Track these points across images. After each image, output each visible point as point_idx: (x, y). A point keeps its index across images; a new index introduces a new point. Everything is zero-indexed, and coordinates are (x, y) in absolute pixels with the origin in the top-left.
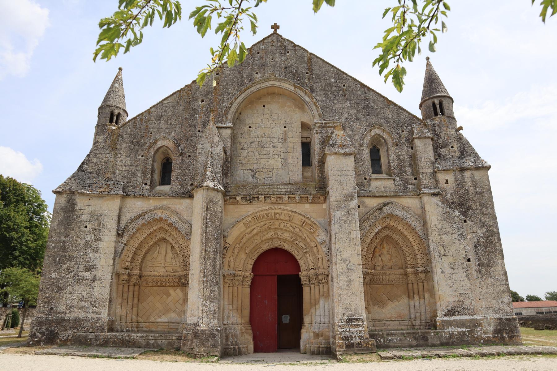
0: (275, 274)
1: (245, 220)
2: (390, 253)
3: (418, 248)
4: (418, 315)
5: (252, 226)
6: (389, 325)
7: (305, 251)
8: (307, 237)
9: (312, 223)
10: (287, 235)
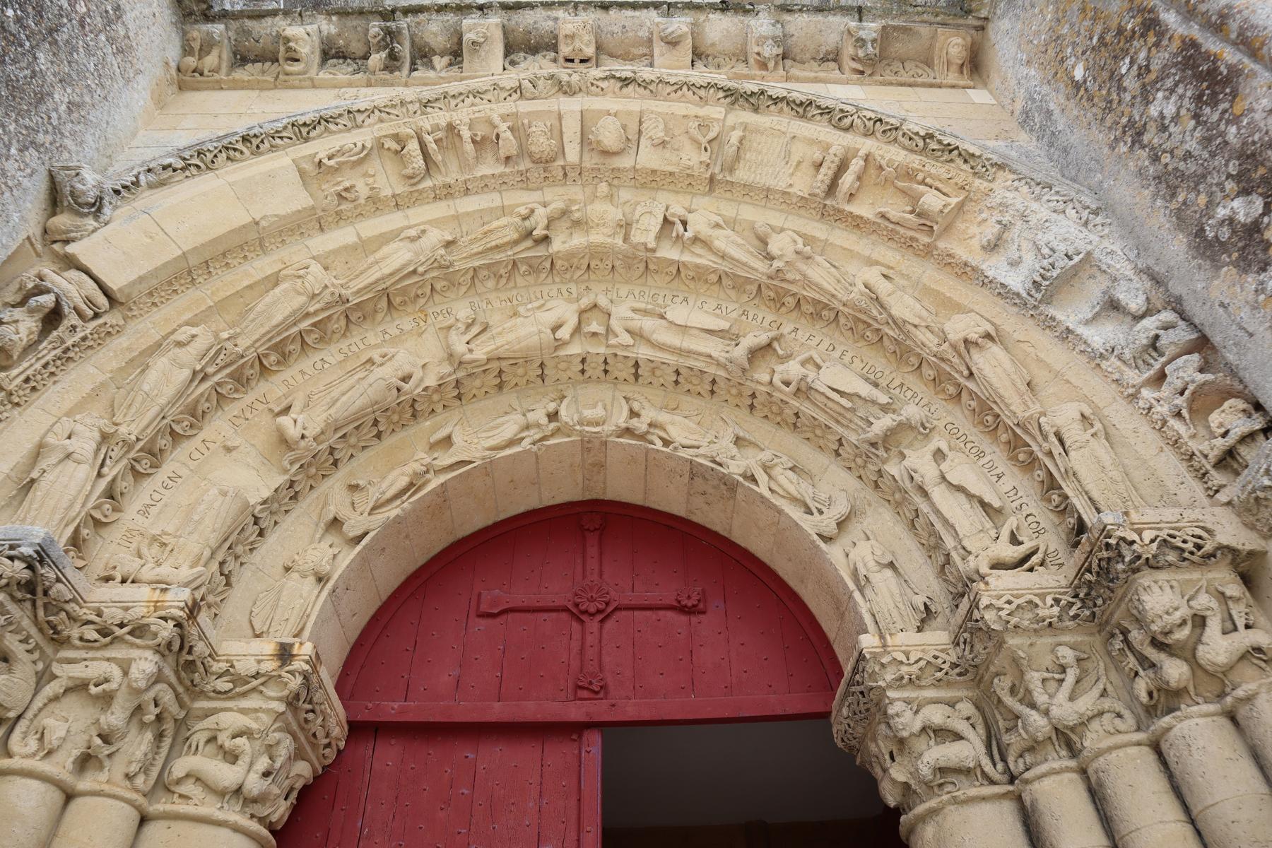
0: (575, 712)
1: (321, 147)
5: (376, 203)
7: (883, 423)
8: (883, 287)
9: (915, 161)
10: (694, 324)
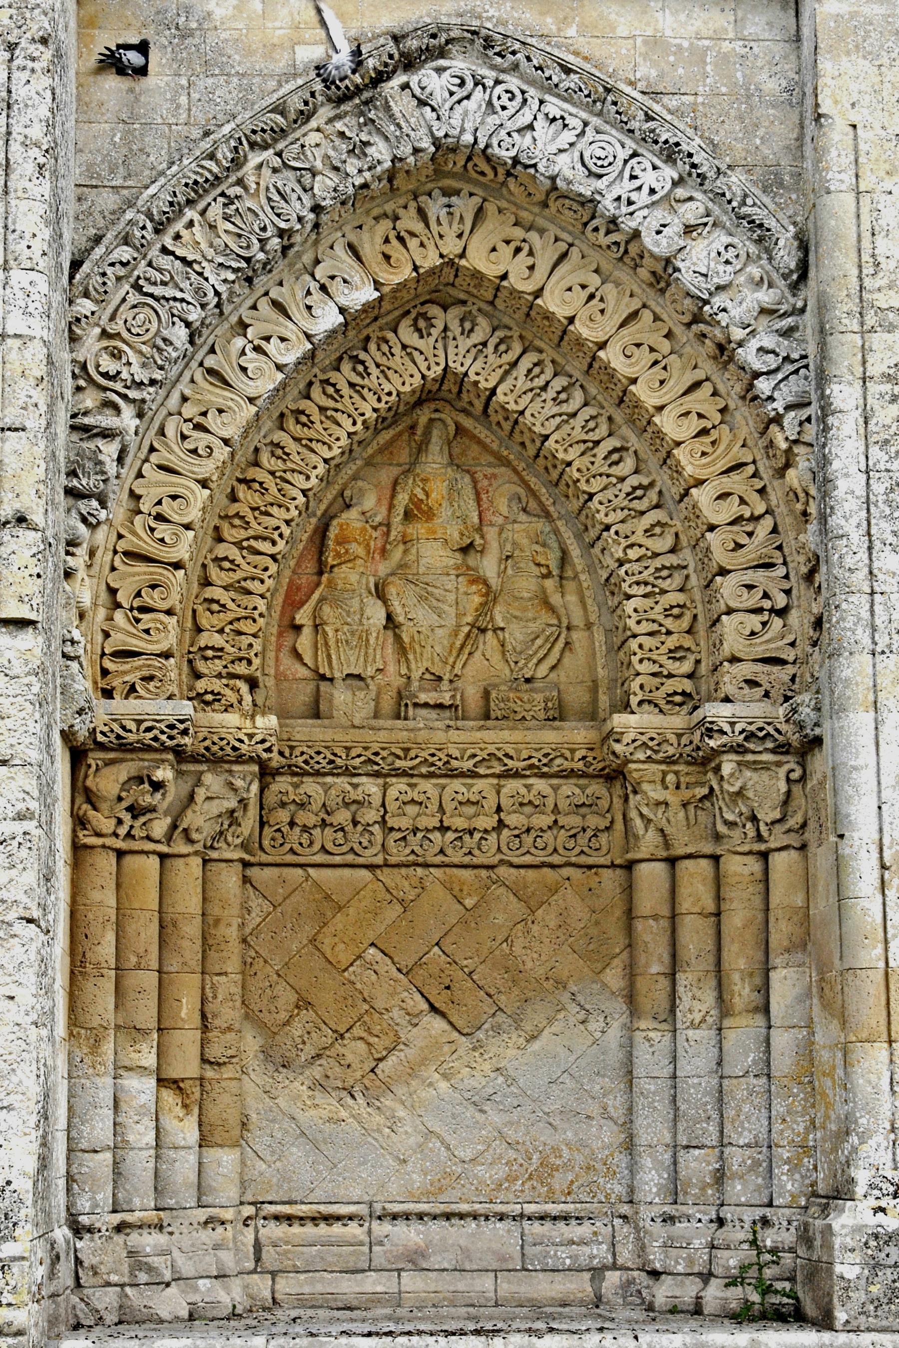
2: (489, 566)
3: (731, 509)
4: (697, 1165)
6: (415, 1261)
